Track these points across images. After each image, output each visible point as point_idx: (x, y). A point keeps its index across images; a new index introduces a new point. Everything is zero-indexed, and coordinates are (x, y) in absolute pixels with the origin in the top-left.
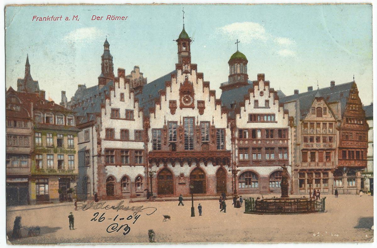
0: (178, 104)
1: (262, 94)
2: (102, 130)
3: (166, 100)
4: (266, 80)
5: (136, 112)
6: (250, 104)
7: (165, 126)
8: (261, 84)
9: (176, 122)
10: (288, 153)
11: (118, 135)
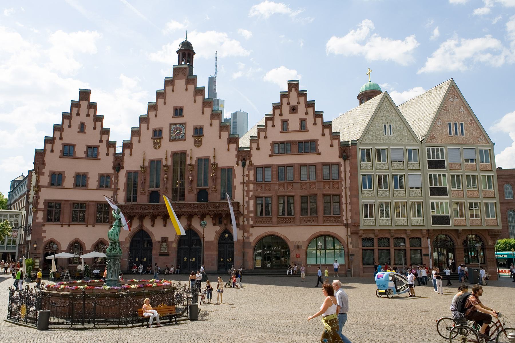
0: (166, 134)
1: (294, 110)
2: (43, 174)
3: (148, 129)
4: (301, 88)
5: (103, 149)
6: (273, 126)
7: (142, 167)
8: (294, 95)
9: (159, 161)
10: (340, 202)
11: (69, 181)
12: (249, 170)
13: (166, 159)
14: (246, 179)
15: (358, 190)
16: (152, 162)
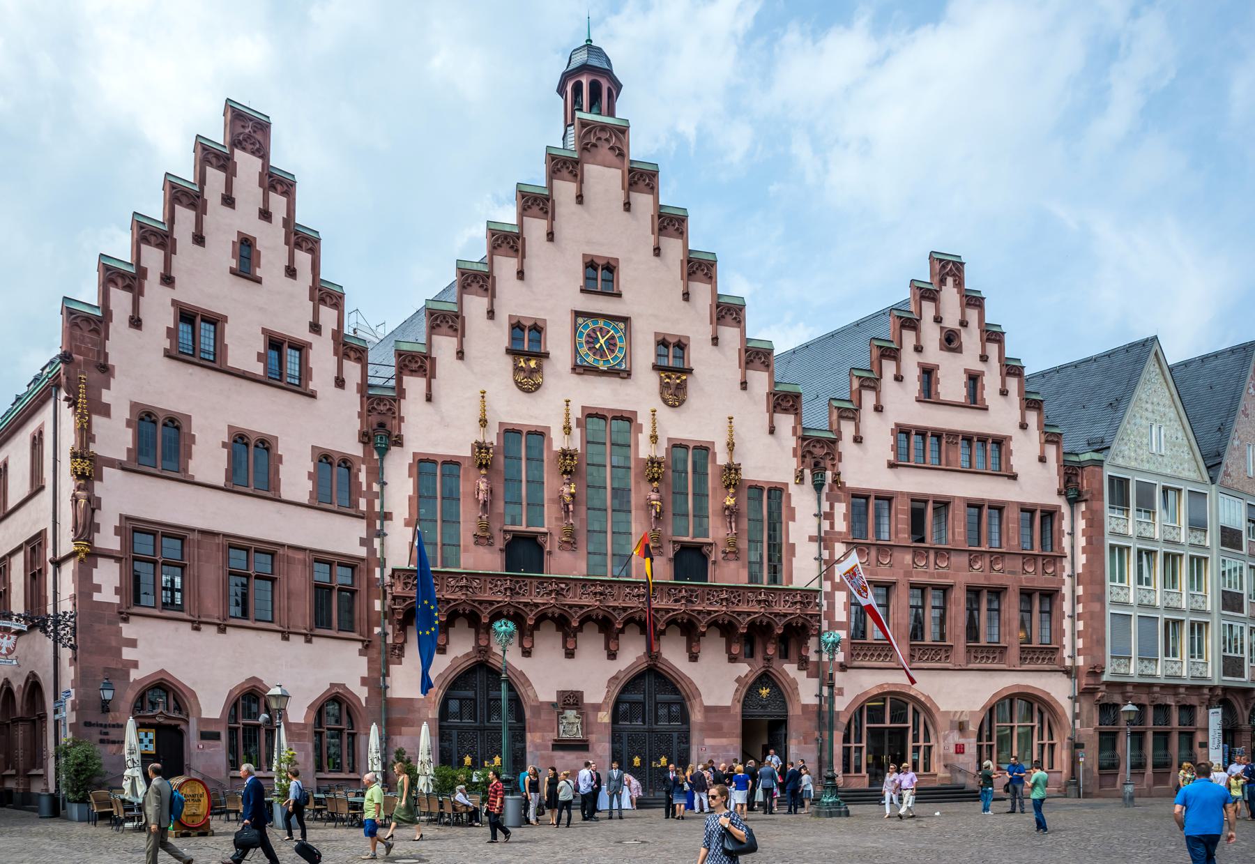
7: (480, 447)
9: (539, 435)
12: (832, 500)
13: (567, 430)
14: (826, 525)
15: (1103, 583)
16: (510, 432)
